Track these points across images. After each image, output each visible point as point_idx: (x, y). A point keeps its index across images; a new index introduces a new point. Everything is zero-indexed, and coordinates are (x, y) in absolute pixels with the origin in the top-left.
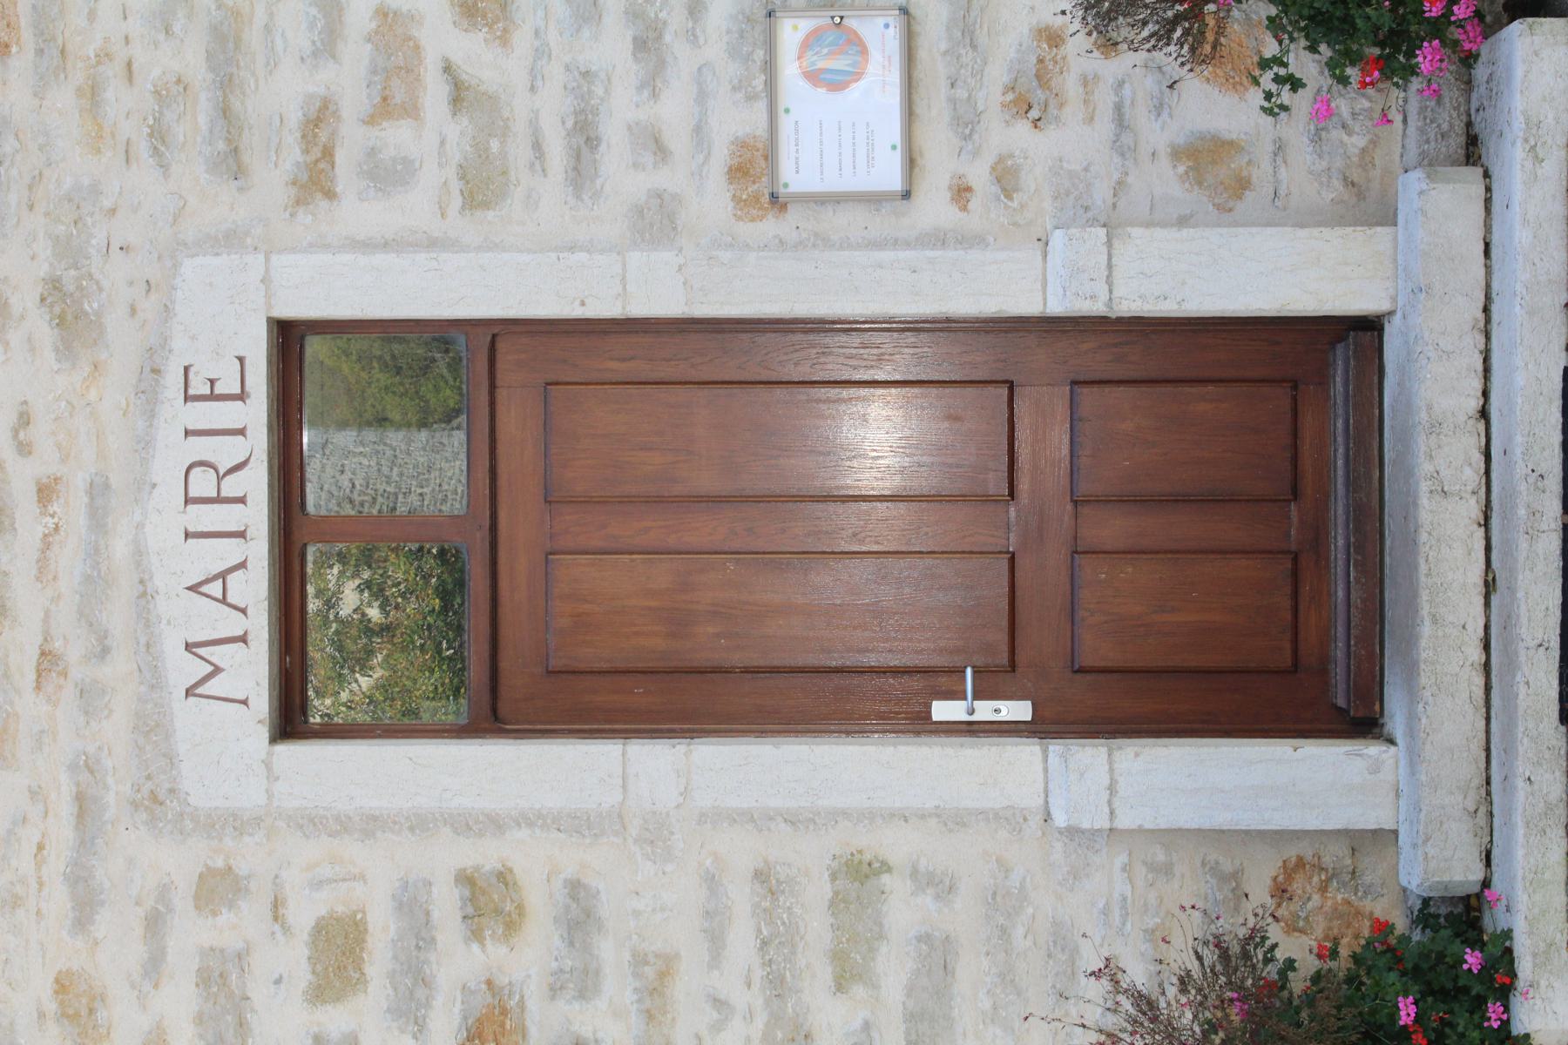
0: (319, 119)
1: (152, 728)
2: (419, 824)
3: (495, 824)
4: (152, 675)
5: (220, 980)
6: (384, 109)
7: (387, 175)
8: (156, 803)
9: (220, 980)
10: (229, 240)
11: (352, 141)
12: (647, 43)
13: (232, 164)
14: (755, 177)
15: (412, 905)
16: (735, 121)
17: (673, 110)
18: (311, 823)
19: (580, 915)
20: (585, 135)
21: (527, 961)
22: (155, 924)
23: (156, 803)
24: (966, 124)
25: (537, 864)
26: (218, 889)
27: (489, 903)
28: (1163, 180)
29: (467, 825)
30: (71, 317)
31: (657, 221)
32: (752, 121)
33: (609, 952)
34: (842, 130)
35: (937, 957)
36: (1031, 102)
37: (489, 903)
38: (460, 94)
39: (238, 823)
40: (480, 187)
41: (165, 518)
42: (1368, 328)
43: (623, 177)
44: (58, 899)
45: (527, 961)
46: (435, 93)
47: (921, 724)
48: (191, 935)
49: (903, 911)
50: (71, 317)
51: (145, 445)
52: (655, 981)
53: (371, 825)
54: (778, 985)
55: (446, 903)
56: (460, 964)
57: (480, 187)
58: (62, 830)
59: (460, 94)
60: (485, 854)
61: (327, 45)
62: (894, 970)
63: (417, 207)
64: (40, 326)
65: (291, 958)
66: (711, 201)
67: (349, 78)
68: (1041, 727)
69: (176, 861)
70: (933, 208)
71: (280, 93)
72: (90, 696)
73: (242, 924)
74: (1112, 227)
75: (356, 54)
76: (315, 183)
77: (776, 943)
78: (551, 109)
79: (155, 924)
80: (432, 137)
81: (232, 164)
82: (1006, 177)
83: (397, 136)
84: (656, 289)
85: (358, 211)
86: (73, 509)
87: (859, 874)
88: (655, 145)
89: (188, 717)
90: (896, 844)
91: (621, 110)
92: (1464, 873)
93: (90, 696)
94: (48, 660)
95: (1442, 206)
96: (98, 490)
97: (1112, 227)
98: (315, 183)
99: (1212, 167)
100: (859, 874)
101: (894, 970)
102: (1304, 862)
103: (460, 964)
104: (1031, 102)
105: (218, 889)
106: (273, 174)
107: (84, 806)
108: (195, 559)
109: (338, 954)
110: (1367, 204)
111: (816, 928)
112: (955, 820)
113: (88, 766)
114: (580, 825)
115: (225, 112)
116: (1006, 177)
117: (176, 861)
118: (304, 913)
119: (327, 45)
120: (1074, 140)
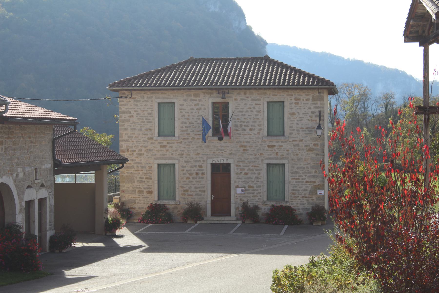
0: (240, 166)
1: (211, 158)
2: (207, 170)
3: (207, 174)
4: (214, 158)
5: (199, 161)
6: (240, 169)
7: (237, 169)
8: (208, 158)
9: (199, 161)
10: (234, 161)
11: (239, 167)
12: (244, 181)
13: (238, 162)
14: (237, 187)
15: (203, 170)
16: (240, 186)
17: (240, 183)
18: (207, 165)
19: (202, 178)
20: (239, 178)
21: (200, 175)
22: (202, 158)
23: (208, 158)
24: (240, 197)
25: (205, 176)
26: (204, 161)
27: (203, 174)
28: (237, 206)
29: (207, 173)
30: (231, 154)
31: (235, 182)
32: (240, 186)
33: (201, 179)
34: (239, 190)
35: (201, 195)
36: (241, 200)
37: (203, 174)
38: (241, 173)
39: (207, 162)
40: (237, 173)
41: (221, 158)
42: (230, 216)
43: (237, 180)
44: (203, 153)
45: (200, 175)
46: (241, 171)
47: (212, 194)
48: (201, 160)
49: (203, 193)
50: (231, 154)
51: (224, 157)
52: (200, 182)
53: (207, 168)
54: (199, 187)
55: (203, 172)
56: (200, 172)
57: (237, 173)
58: (206, 153)
59: (241, 173)
60: (205, 174)
61: (243, 166)
62: (200, 193)
63: (236, 170)
64: (230, 152)
65: (200, 165)
66: (236, 184)
67: (242, 167)
68: (211, 200)
69: (205, 159)
70: (236, 195)
71: (241, 164)
72: (213, 155)
73: (202, 162)
74: (235, 204)
75: (243, 168)
76: (237, 166)
77: (201, 187)
78: (240, 177)
79: (202, 158)
80: (239, 171)
81: (238, 162)
82: (237, 198)
83: (239, 170)
84: (232, 182)
85: (236, 168)
86: (222, 154)
87: (204, 191)
88: (239, 182)
89: (212, 159)
90: (206, 193)
91: (240, 180)
92: (205, 219)
93: (213, 155)
94: (214, 153)
95: (235, 218)
96: (222, 155)
97: (235, 204)
98: (237, 166)
99: (238, 208)
100: (204, 191)
101: (200, 193)
102: (205, 212)
103: (200, 172)
104: (241, 200)
105: (204, 161)
106: (237, 164)
107: (208, 154)
108: (220, 160)
109: (201, 166)
110: (236, 215)
111: (202, 189)
112: (207, 196)
113: (209, 155)
114: (207, 178)
115: (240, 161)
116: (237, 198)
117: (205, 159)
118: (202, 165)
119: (243, 166)
120: (239, 202)
